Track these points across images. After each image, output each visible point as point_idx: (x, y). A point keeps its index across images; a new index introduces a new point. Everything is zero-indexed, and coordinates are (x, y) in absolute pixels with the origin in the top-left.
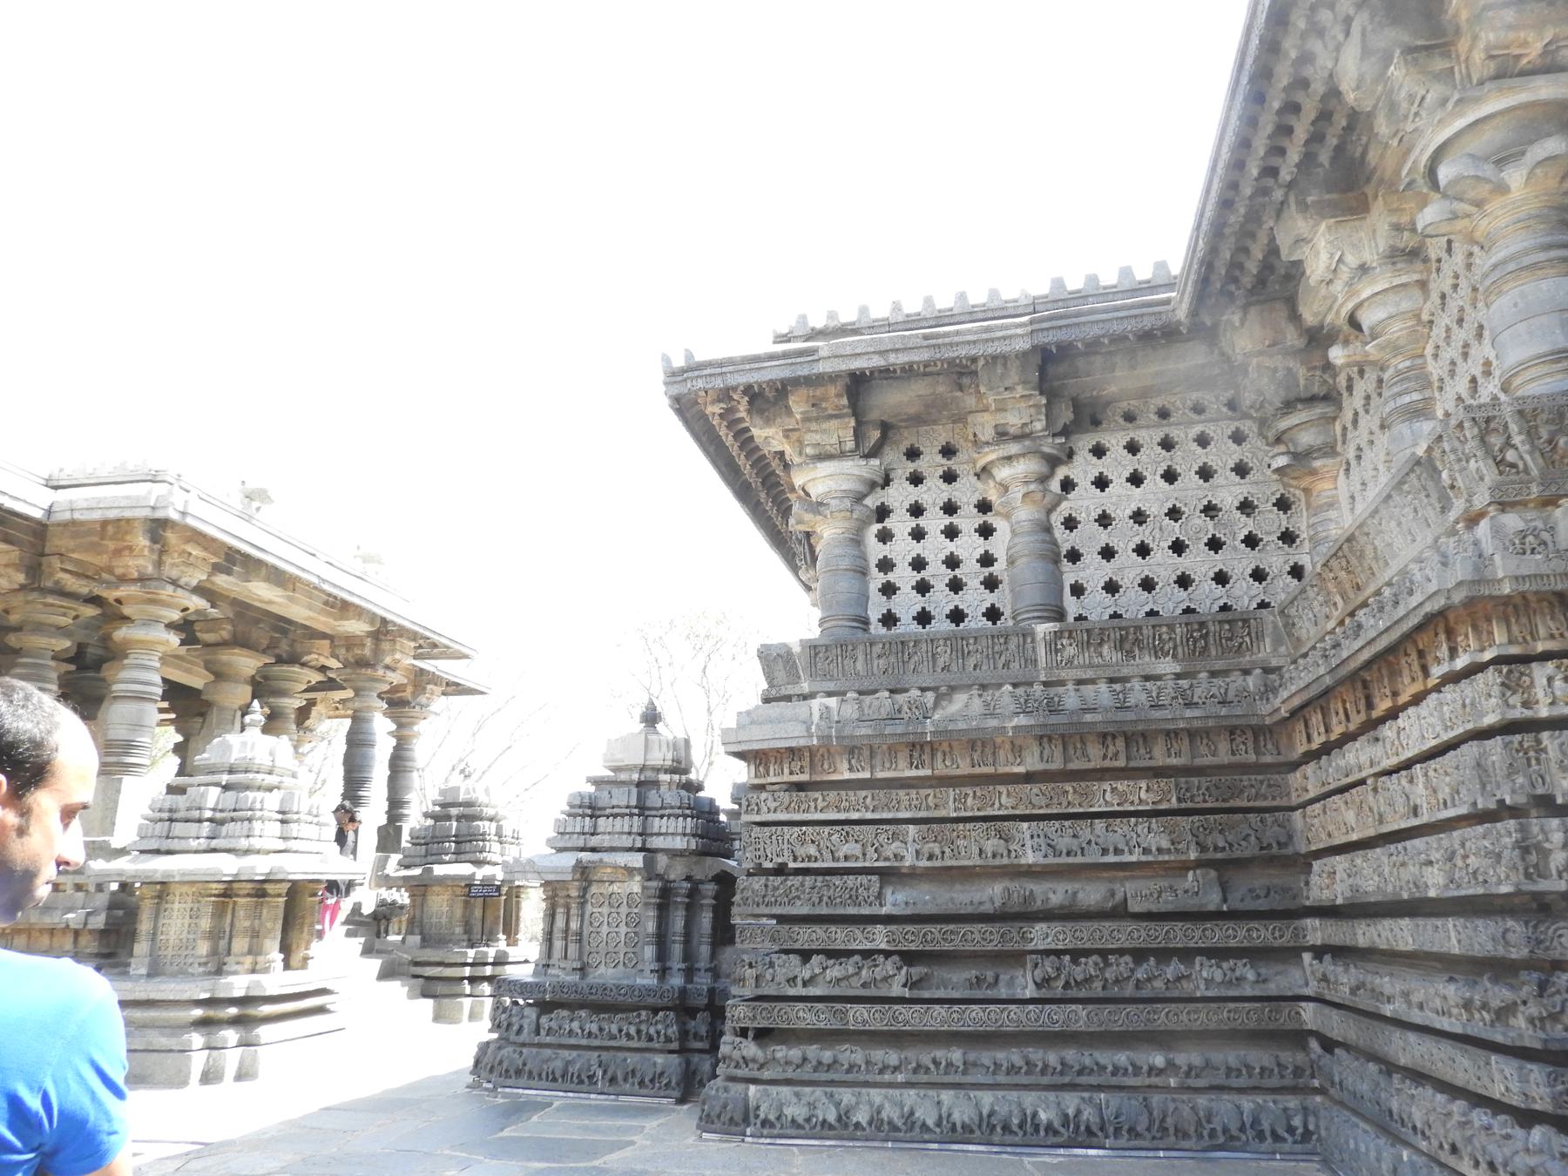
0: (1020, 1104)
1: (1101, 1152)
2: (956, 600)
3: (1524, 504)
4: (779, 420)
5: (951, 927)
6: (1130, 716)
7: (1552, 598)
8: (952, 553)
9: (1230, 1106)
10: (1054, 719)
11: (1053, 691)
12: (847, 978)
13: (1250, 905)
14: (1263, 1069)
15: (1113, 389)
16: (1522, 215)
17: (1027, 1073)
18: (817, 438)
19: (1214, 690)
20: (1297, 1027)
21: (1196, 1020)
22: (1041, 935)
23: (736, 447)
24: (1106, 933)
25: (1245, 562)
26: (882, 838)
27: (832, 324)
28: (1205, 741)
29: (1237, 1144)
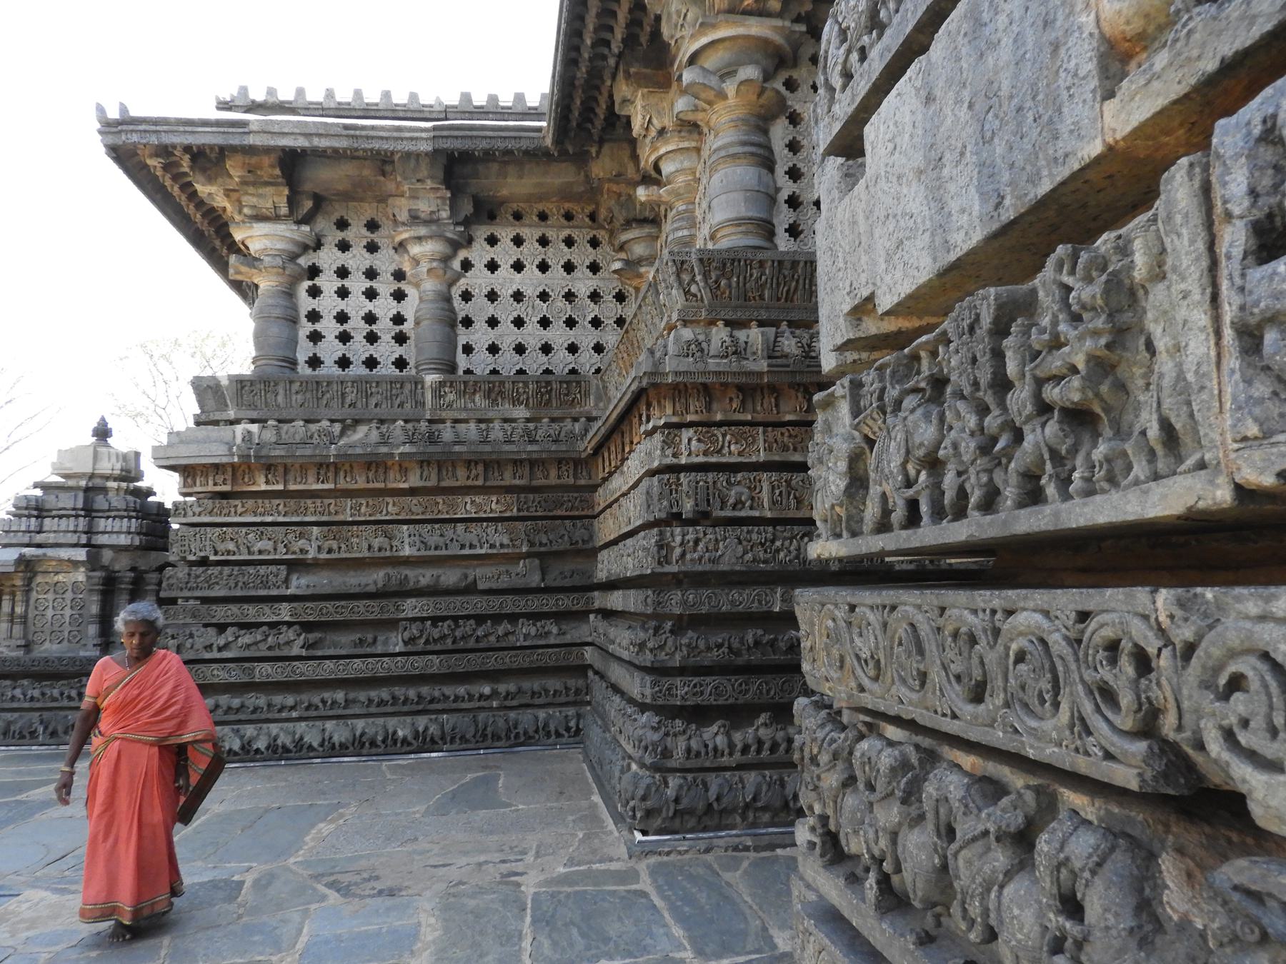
0: (385, 727)
1: (440, 754)
2: (372, 350)
3: (698, 322)
4: (220, 180)
5: (343, 603)
6: (488, 448)
7: (700, 388)
10: (431, 449)
11: (435, 427)
12: (256, 643)
13: (559, 583)
14: (555, 691)
15: (504, 192)
16: (734, 117)
18: (254, 201)
19: (552, 432)
20: (580, 662)
22: (411, 607)
23: (183, 198)
24: (458, 604)
25: (590, 338)
27: (271, 100)
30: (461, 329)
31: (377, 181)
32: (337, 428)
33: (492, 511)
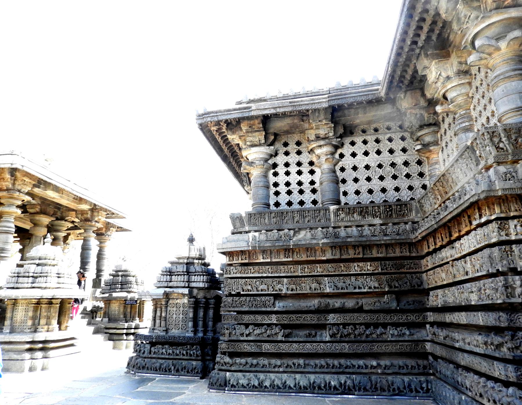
0: (324, 379)
1: (354, 396)
2: (301, 197)
3: (506, 162)
4: (237, 132)
7: (516, 197)
8: (300, 180)
9: (400, 379)
11: (336, 230)
12: (262, 334)
13: (407, 307)
14: (412, 366)
15: (358, 121)
17: (327, 368)
18: (251, 139)
19: (394, 230)
21: (388, 349)
22: (332, 318)
23: (222, 142)
24: (355, 317)
25: (405, 184)
26: (275, 283)
28: (391, 248)
29: (403, 393)
30: (341, 185)
31: (301, 124)
32: (292, 232)
33: (368, 270)
